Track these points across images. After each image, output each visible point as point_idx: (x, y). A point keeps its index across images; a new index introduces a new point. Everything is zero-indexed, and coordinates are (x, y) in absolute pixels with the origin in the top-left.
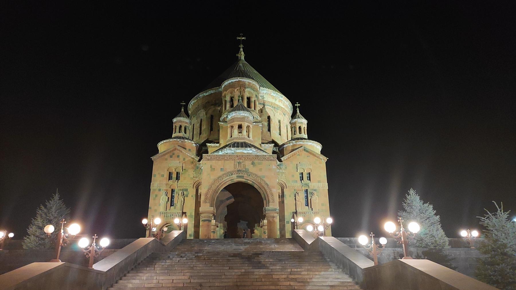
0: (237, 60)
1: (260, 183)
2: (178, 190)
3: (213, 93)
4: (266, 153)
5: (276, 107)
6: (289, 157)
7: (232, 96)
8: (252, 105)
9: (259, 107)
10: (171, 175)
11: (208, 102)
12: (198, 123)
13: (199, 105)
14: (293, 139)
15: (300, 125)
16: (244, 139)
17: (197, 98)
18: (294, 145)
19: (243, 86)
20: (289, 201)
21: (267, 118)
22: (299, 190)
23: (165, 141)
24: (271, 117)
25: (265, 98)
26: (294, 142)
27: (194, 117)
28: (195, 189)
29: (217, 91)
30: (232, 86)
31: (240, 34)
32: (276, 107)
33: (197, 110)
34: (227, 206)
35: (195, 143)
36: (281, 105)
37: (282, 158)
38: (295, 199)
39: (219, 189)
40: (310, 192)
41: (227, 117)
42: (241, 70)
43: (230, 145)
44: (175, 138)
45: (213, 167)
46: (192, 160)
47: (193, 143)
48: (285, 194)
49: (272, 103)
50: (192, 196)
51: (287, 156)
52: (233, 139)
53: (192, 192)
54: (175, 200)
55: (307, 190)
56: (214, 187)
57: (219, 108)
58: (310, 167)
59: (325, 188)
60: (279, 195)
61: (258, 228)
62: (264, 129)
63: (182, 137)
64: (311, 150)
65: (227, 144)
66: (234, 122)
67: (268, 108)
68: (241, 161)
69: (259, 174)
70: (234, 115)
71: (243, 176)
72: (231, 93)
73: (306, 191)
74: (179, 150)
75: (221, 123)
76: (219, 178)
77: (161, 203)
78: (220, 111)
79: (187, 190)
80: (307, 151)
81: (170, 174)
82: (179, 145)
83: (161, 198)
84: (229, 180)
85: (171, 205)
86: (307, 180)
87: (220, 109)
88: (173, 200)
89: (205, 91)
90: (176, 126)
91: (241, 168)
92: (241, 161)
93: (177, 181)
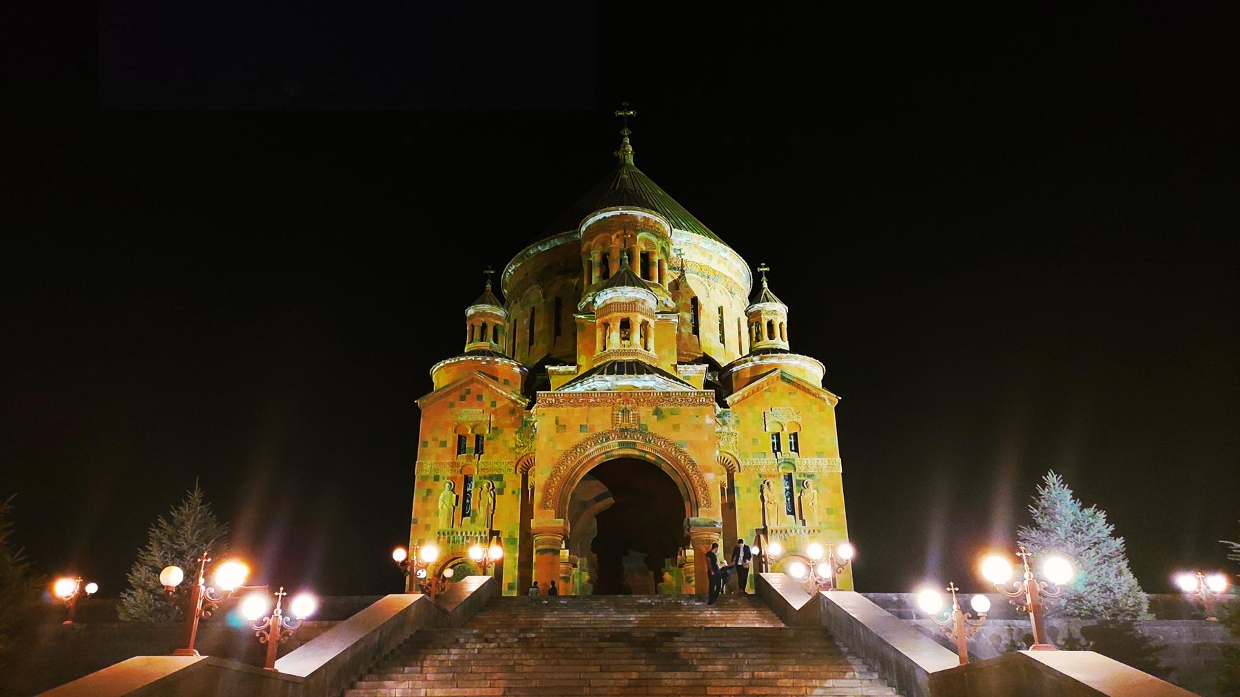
0: (618, 164)
1: (675, 460)
2: (480, 478)
3: (562, 245)
4: (689, 385)
5: (708, 274)
6: (746, 395)
7: (606, 251)
9: (670, 276)
10: (463, 443)
13: (526, 275)
14: (753, 352)
15: (770, 318)
16: (634, 353)
17: (523, 258)
18: (756, 368)
20: (745, 502)
21: (689, 302)
22: (770, 476)
23: (448, 362)
24: (701, 300)
25: (684, 254)
27: (516, 302)
28: (521, 475)
30: (603, 226)
33: (522, 287)
34: (597, 516)
35: (519, 366)
36: (723, 269)
37: (728, 400)
38: (762, 498)
39: (576, 475)
40: (797, 480)
41: (594, 301)
42: (625, 188)
43: (602, 368)
44: (471, 353)
45: (561, 423)
47: (513, 366)
48: (737, 484)
50: (513, 492)
51: (740, 392)
52: (608, 355)
53: (513, 482)
54: (473, 501)
57: (575, 281)
58: (795, 420)
59: (834, 471)
60: (722, 489)
61: (671, 568)
62: (683, 330)
63: (489, 351)
64: (799, 380)
65: (595, 366)
66: (610, 312)
67: (691, 278)
68: (629, 406)
69: (674, 437)
70: (609, 296)
71: (635, 443)
72: (603, 244)
75: (579, 316)
76: (576, 447)
77: (440, 507)
79: (500, 478)
80: (789, 381)
81: (461, 440)
82: (482, 371)
83: (441, 497)
84: (596, 453)
85: (464, 515)
86: (790, 452)
87: (578, 282)
88: (468, 501)
89: (543, 240)
90: (473, 326)
91: (631, 423)
92: (629, 406)
93: (477, 455)
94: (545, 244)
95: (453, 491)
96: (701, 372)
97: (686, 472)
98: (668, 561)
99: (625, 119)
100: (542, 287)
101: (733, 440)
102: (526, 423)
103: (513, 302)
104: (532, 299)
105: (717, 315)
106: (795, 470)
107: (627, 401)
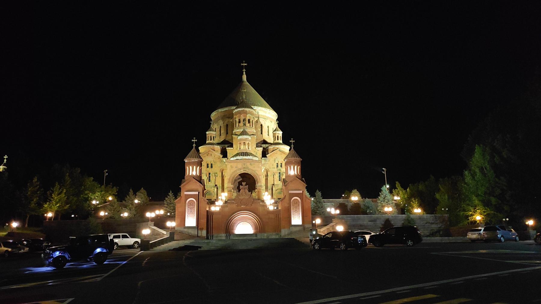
5: (265, 118)
8: (251, 124)
11: (224, 116)
13: (218, 117)
15: (278, 135)
20: (270, 178)
24: (263, 125)
27: (216, 123)
29: (230, 109)
30: (240, 113)
32: (266, 118)
34: (238, 182)
37: (267, 156)
44: (209, 144)
45: (232, 166)
46: (219, 157)
48: (268, 174)
50: (220, 176)
54: (211, 178)
55: (280, 172)
56: (233, 176)
57: (231, 120)
66: (241, 141)
69: (254, 169)
70: (241, 137)
71: (246, 170)
72: (239, 117)
73: (280, 173)
76: (235, 171)
78: (233, 122)
79: (217, 173)
80: (281, 151)
81: (208, 164)
85: (209, 181)
94: (223, 109)
96: (261, 149)
97: (255, 176)
100: (223, 121)
102: (222, 161)
104: (220, 124)
107: (245, 162)
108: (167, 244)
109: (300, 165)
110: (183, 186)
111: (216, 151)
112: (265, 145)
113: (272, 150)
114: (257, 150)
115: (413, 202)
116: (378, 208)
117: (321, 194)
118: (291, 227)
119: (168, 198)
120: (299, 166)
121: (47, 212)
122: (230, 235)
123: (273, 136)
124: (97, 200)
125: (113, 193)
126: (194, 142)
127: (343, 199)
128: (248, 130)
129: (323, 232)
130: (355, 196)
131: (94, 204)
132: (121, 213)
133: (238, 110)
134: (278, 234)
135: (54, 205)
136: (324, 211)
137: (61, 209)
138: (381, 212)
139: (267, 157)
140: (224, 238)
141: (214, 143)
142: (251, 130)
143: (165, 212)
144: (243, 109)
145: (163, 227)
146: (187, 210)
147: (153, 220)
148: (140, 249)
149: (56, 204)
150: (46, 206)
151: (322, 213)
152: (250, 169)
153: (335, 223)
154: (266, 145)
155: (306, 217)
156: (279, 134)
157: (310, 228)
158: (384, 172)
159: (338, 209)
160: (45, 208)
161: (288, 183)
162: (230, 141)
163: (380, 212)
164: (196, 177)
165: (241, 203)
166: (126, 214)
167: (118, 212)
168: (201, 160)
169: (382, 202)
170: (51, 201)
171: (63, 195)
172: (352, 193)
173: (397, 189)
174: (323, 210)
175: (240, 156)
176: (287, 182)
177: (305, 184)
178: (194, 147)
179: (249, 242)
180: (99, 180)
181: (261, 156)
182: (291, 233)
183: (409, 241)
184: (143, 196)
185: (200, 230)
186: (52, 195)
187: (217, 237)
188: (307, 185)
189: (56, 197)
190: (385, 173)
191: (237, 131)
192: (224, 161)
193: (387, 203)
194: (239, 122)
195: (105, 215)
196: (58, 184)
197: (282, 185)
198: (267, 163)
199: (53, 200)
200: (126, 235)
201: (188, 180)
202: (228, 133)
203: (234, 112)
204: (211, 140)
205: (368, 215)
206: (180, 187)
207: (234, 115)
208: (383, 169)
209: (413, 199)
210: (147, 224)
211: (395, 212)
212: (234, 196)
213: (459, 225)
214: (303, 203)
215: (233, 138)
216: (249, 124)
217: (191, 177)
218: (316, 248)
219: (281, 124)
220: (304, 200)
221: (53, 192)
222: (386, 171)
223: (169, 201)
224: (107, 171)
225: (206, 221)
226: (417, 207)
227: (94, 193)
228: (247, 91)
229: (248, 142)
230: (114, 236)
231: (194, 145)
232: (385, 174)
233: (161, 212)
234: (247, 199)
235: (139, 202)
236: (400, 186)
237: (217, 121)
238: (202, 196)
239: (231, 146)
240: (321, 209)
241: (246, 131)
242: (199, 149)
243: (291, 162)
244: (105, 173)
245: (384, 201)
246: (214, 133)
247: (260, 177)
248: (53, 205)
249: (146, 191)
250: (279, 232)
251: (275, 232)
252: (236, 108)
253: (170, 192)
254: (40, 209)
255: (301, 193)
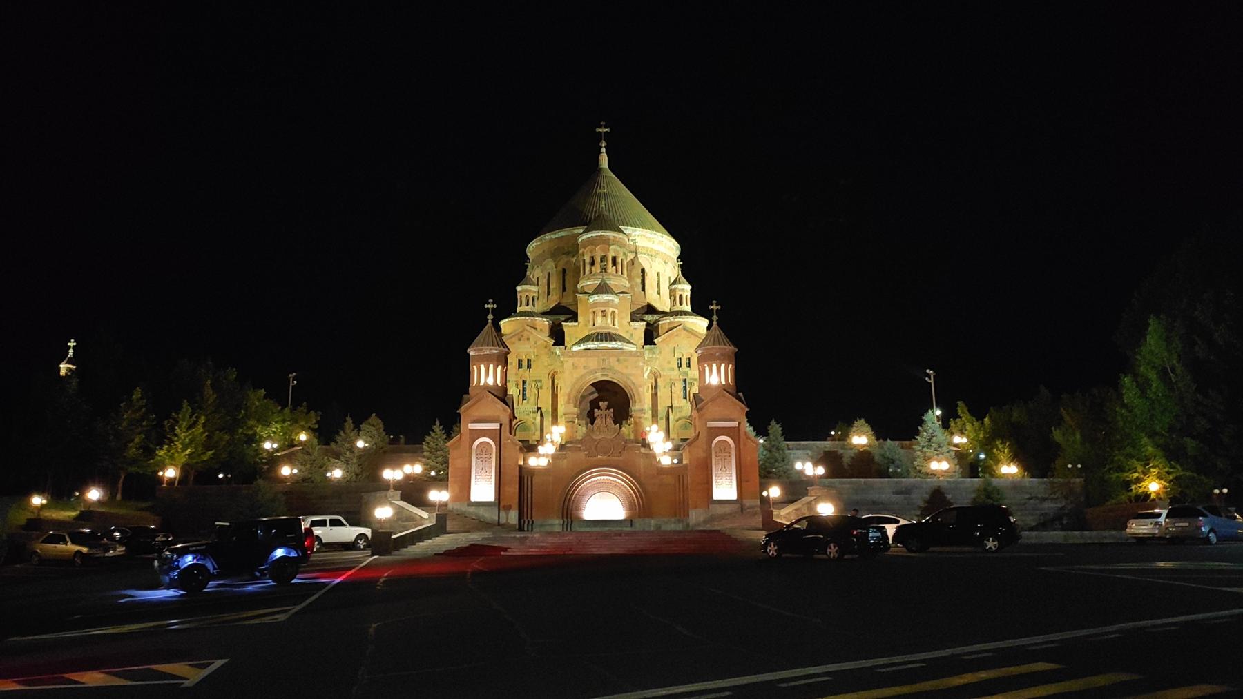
3: (566, 236)
5: (652, 254)
12: (545, 278)
13: (544, 252)
15: (680, 293)
16: (609, 328)
19: (607, 242)
20: (663, 393)
21: (640, 271)
23: (510, 319)
24: (647, 270)
26: (671, 318)
27: (538, 267)
29: (570, 233)
30: (592, 242)
31: (602, 123)
32: (653, 254)
37: (656, 341)
45: (575, 365)
46: (545, 343)
48: (658, 384)
49: (648, 248)
52: (596, 329)
53: (547, 383)
56: (577, 387)
57: (574, 260)
64: (693, 330)
66: (596, 307)
67: (641, 257)
68: (605, 358)
69: (625, 371)
70: (596, 298)
72: (591, 252)
73: (685, 381)
74: (529, 331)
79: (540, 381)
80: (687, 331)
81: (520, 361)
82: (529, 324)
85: (523, 399)
90: (521, 297)
94: (555, 234)
95: (517, 387)
96: (643, 325)
98: (624, 422)
99: (603, 135)
100: (555, 261)
101: (658, 362)
103: (536, 266)
105: (656, 277)
106: (688, 376)
107: (604, 355)
108: (430, 541)
109: (734, 363)
110: (465, 411)
111: (539, 330)
112: (650, 316)
113: (667, 327)
114: (632, 328)
115: (998, 449)
116: (915, 463)
117: (781, 429)
118: (713, 504)
119: (432, 438)
120: (730, 366)
121: (163, 468)
122: (572, 522)
123: (670, 297)
124: (273, 441)
125: (309, 424)
126: (490, 311)
127: (832, 440)
128: (611, 282)
129: (787, 516)
130: (860, 435)
131: (267, 450)
132: (326, 471)
133: (589, 235)
134: (682, 521)
135: (180, 450)
136: (788, 470)
137: (195, 461)
138: (923, 471)
139: (655, 344)
140: (558, 529)
141: (535, 313)
142: (618, 281)
143: (425, 469)
144: (600, 233)
145: (422, 503)
146: (473, 464)
147: (398, 486)
148: (370, 551)
149: (184, 450)
150: (161, 453)
151: (785, 473)
152: (616, 371)
153: (814, 498)
154: (653, 317)
155: (747, 482)
156: (683, 290)
157: (756, 506)
158: (930, 378)
159: (822, 465)
160: (159, 458)
161: (707, 404)
162: (571, 308)
163: (920, 471)
164: (495, 390)
165: (596, 448)
166: (337, 474)
167: (321, 467)
168: (506, 350)
169: (925, 449)
170: (173, 442)
171: (199, 429)
172: (854, 429)
173: (961, 417)
174: (788, 467)
175: (593, 341)
176: (703, 400)
177: (743, 406)
178: (489, 321)
179: (615, 538)
180: (278, 395)
181: (643, 341)
182: (712, 519)
183: (988, 540)
184: (375, 432)
185: (505, 509)
186: (176, 429)
187: (541, 526)
188: (747, 409)
189: (183, 434)
190: (932, 381)
191: (587, 283)
192: (558, 353)
193: (936, 452)
194: (592, 263)
195: (292, 475)
196: (188, 405)
197: (692, 407)
198: (656, 358)
199: (177, 441)
200: (339, 520)
201: (475, 396)
202: (567, 290)
203: (580, 240)
204: (527, 305)
205: (890, 479)
206: (458, 411)
207: (580, 246)
208: (928, 371)
209: (998, 442)
210: (386, 496)
211: (955, 472)
212: (581, 434)
213: (1109, 503)
214: (740, 450)
215: (577, 301)
216: (615, 267)
217: (484, 389)
218: (771, 553)
219: (689, 265)
220: (742, 447)
221: (178, 422)
222: (934, 377)
223: (434, 443)
224: (295, 376)
225: (517, 490)
226: (1008, 461)
227: (267, 424)
228: (610, 192)
229: (611, 310)
230: (313, 521)
231: (490, 317)
232: (931, 383)
233: (416, 469)
234: (612, 440)
235: (367, 445)
236: (969, 411)
237: (540, 260)
238: (508, 433)
239: (573, 317)
240: (780, 465)
241: (607, 284)
242: (499, 326)
243: (712, 354)
244: (291, 379)
245: (929, 447)
246: (535, 288)
247: (641, 389)
248: (177, 451)
249: (382, 421)
250: (684, 516)
251: (676, 516)
252: (584, 232)
253: (435, 425)
254: (149, 460)
255: (734, 428)
